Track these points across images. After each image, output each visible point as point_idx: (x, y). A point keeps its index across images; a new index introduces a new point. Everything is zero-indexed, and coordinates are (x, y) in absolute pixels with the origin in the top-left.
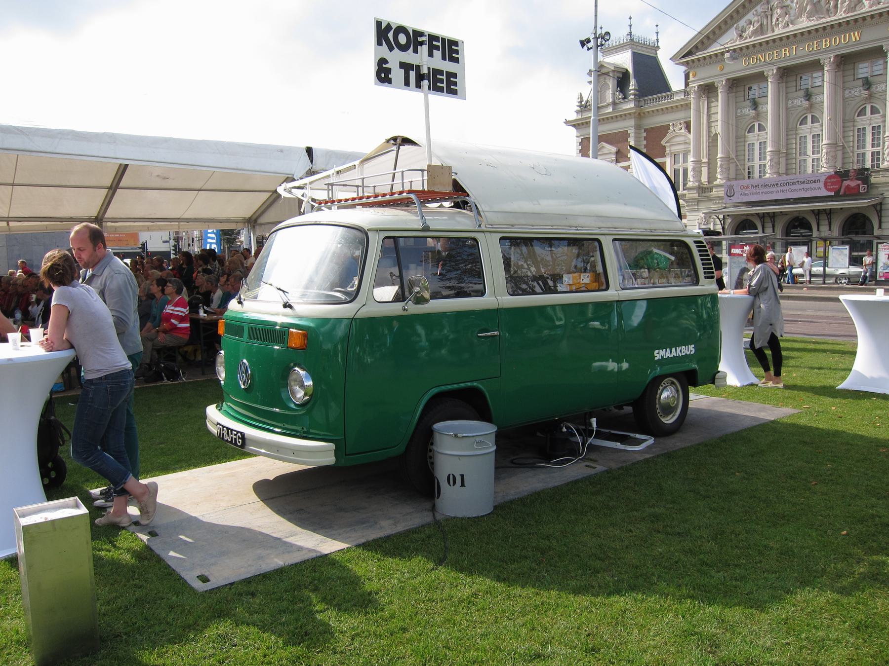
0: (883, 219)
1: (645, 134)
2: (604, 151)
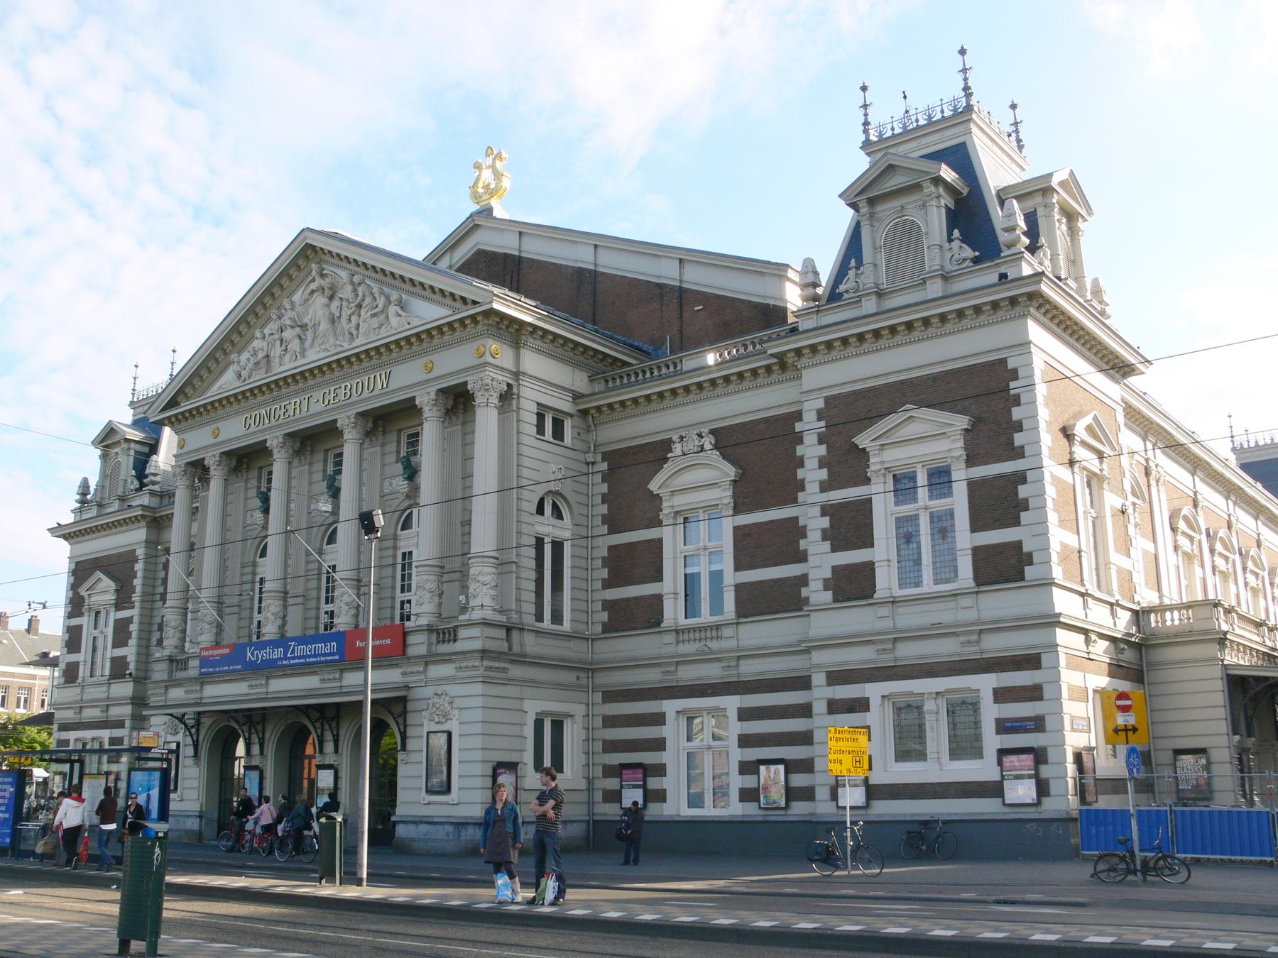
2: (101, 586)
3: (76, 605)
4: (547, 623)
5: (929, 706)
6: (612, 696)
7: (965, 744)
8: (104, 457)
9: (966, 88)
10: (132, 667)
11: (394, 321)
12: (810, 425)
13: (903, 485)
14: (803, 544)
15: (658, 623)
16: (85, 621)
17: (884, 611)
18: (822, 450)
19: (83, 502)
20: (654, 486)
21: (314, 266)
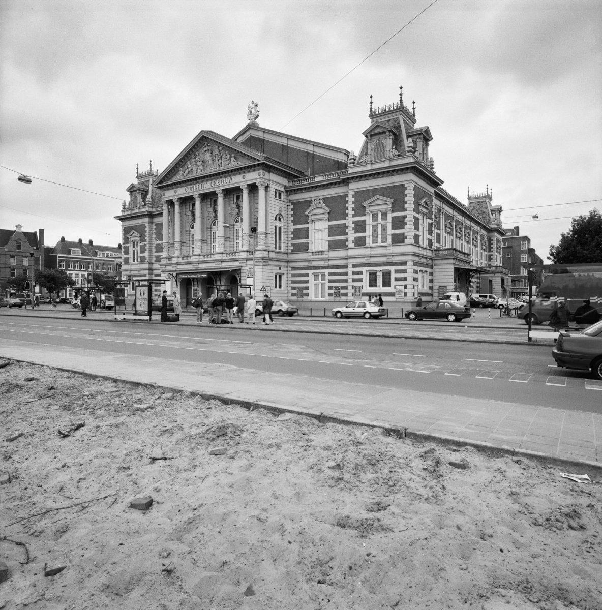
0: (242, 278)
1: (155, 227)
2: (134, 235)
3: (126, 240)
4: (277, 250)
5: (378, 274)
6: (294, 269)
7: (387, 283)
8: (131, 195)
9: (401, 100)
10: (148, 259)
11: (233, 163)
12: (350, 199)
13: (375, 216)
14: (347, 231)
15: (307, 250)
16: (130, 245)
18: (353, 206)
19: (124, 208)
20: (306, 213)
21: (206, 143)
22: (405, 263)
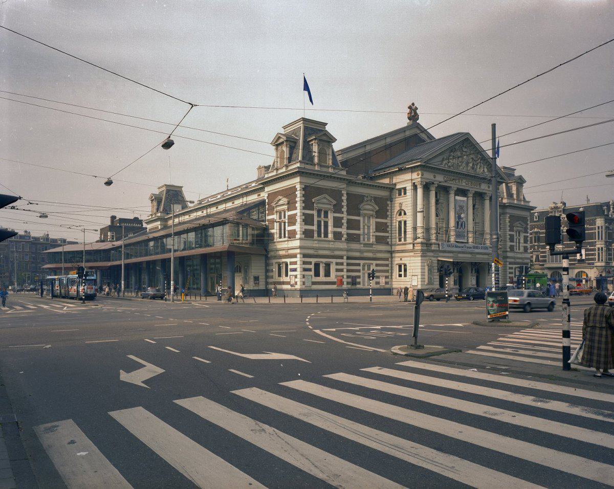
13: (319, 211)
17: (316, 242)
22: (341, 257)
